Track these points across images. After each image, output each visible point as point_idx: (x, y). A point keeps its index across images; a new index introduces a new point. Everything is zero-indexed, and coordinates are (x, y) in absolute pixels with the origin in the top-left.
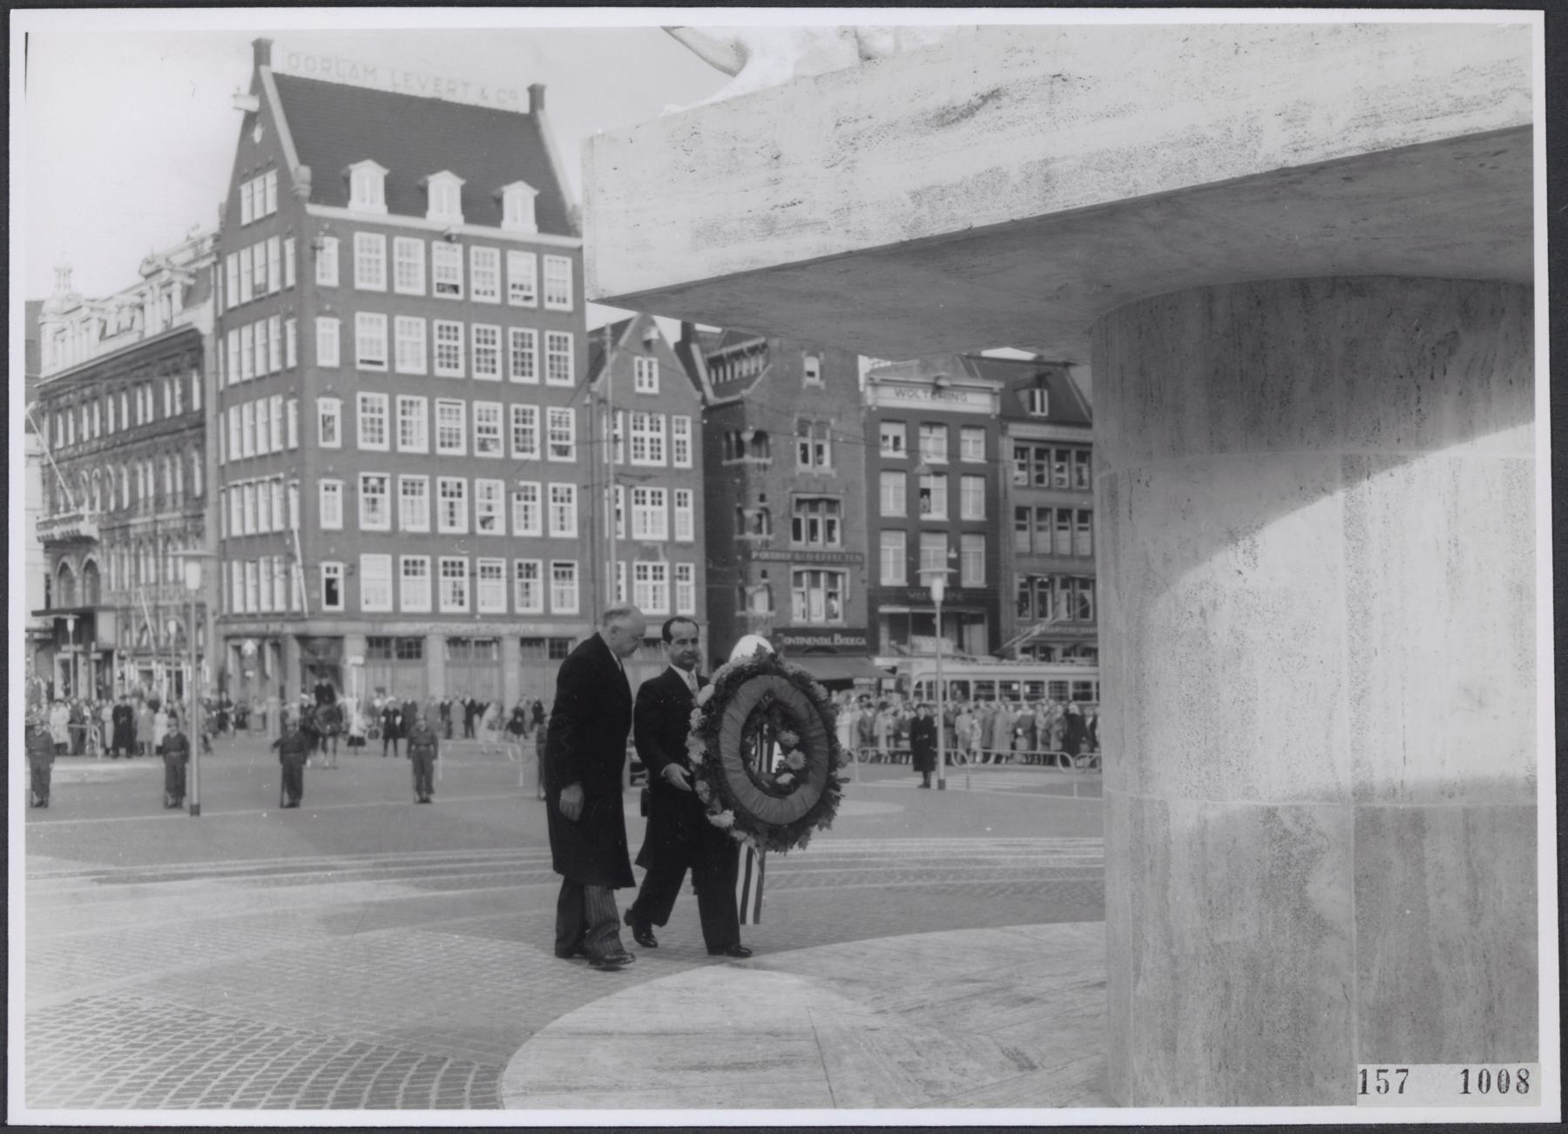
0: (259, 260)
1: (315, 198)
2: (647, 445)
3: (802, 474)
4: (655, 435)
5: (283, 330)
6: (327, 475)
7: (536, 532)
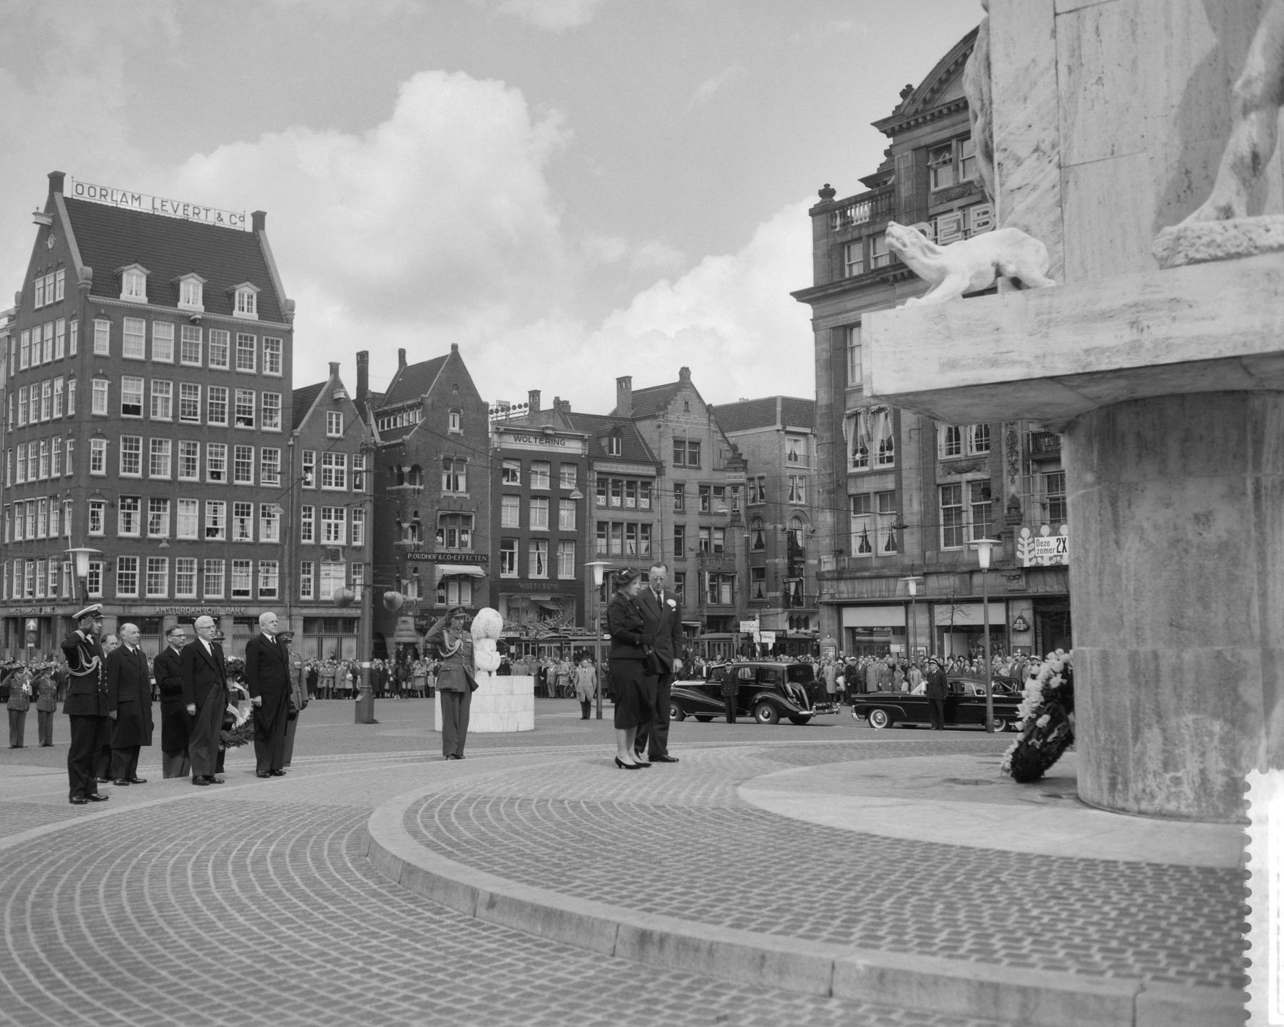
0: (49, 334)
1: (93, 292)
4: (339, 467)
5: (65, 388)
6: (94, 495)
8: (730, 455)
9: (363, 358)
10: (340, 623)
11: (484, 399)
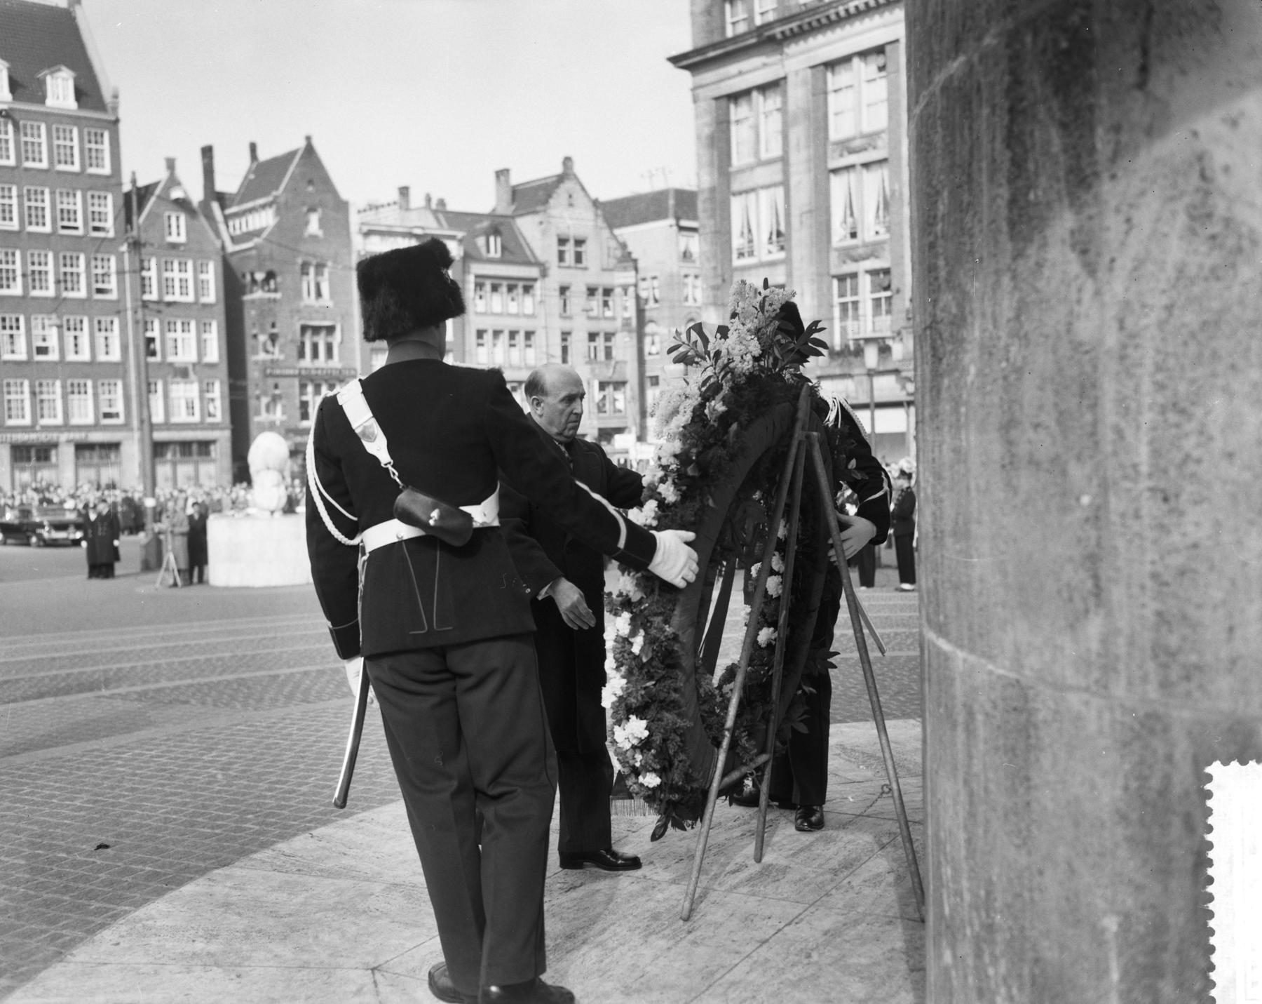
2: (177, 284)
3: (307, 306)
4: (183, 275)
7: (85, 356)
8: (619, 253)
9: (207, 152)
10: (195, 447)
11: (344, 194)
